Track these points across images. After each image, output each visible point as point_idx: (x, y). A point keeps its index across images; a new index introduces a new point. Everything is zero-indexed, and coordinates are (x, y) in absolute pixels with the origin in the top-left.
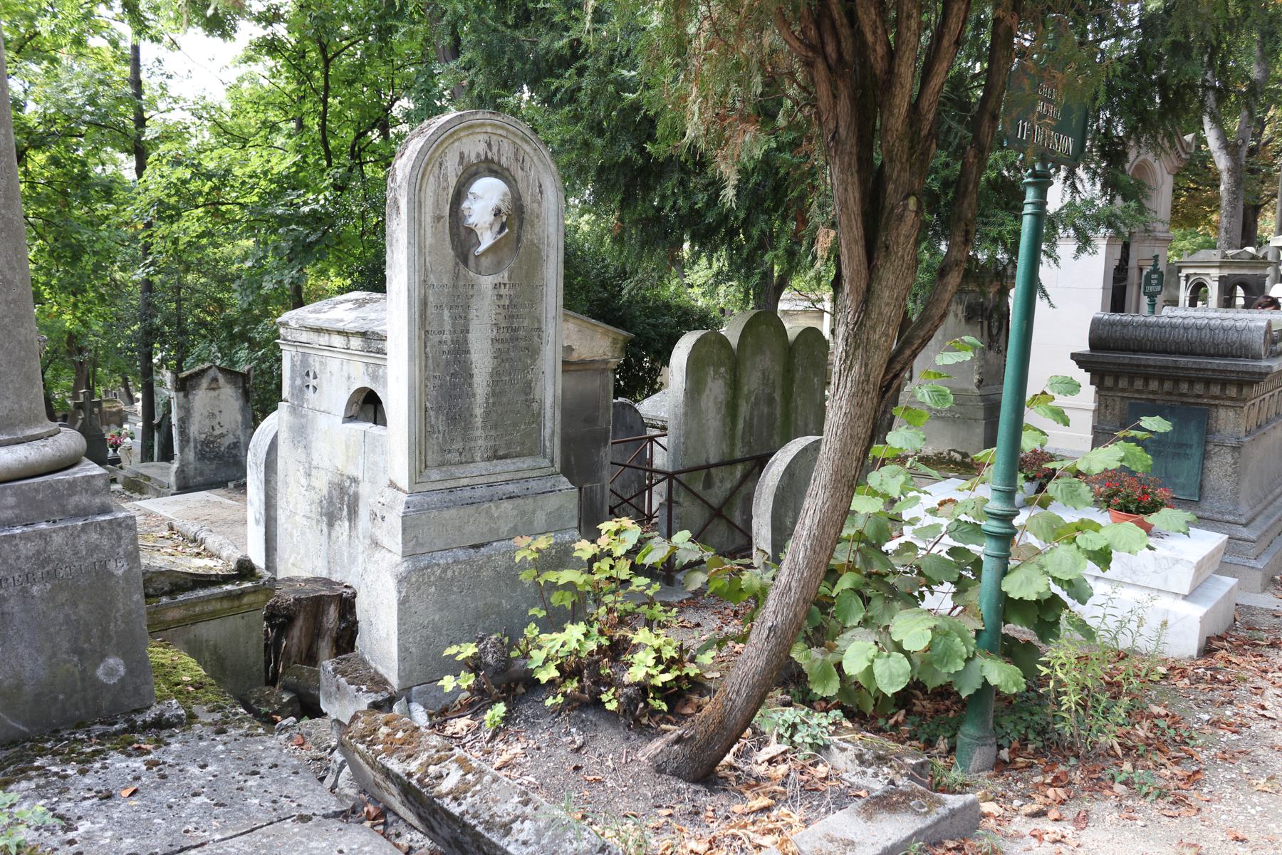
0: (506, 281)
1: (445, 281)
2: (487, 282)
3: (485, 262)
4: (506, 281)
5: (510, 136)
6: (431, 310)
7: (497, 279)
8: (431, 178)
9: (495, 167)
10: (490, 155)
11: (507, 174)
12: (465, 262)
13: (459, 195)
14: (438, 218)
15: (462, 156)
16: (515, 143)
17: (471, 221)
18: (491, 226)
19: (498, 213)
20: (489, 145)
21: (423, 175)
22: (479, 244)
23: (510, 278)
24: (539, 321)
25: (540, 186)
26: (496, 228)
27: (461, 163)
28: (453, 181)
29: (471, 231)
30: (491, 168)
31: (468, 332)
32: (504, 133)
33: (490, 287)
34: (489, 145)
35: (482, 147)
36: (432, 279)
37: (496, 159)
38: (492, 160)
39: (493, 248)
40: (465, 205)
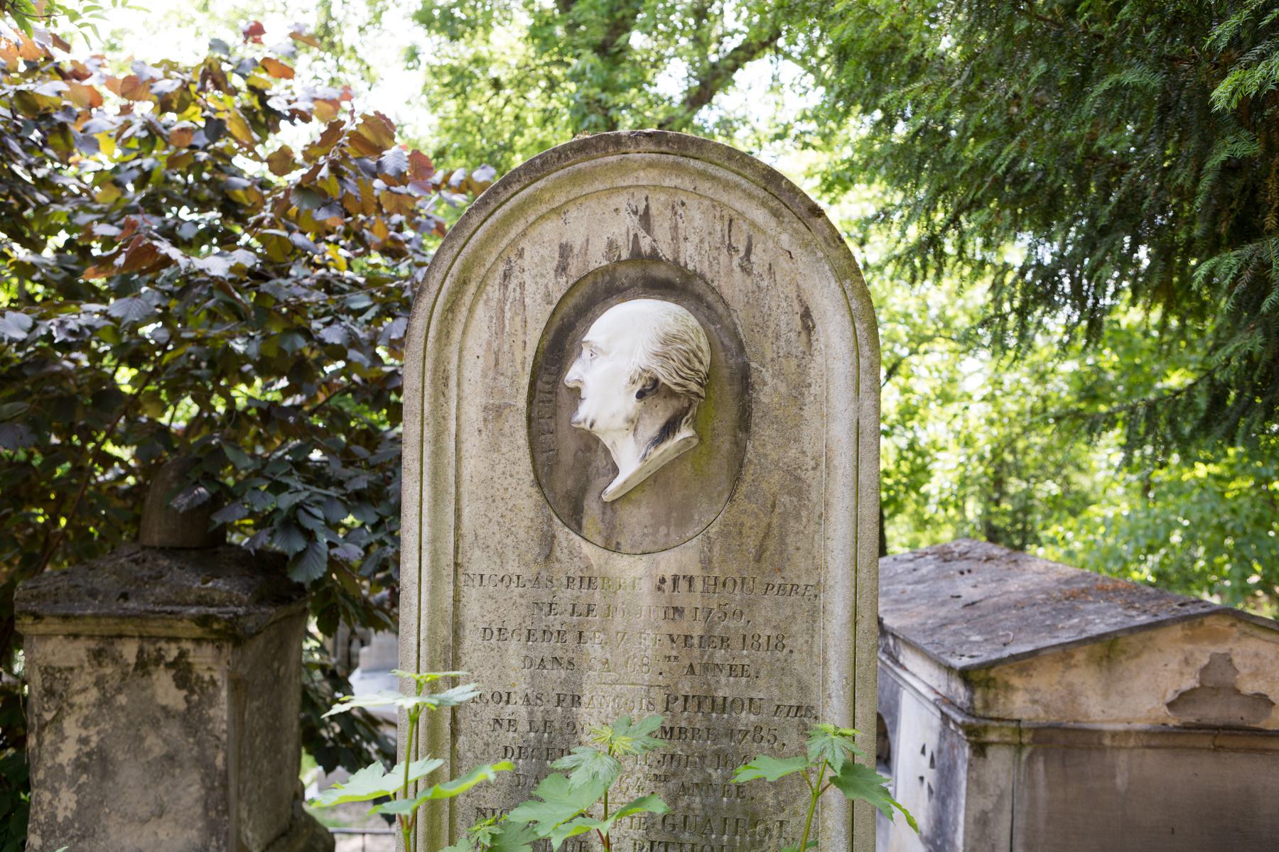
0: (695, 570)
1: (513, 567)
2: (634, 574)
3: (636, 518)
4: (695, 570)
5: (705, 187)
6: (471, 640)
7: (669, 563)
8: (480, 311)
9: (660, 272)
11: (699, 286)
12: (575, 519)
13: (559, 345)
14: (495, 412)
15: (565, 250)
16: (715, 204)
17: (585, 412)
18: (633, 423)
19: (650, 390)
20: (645, 219)
21: (451, 308)
22: (615, 471)
23: (706, 563)
24: (803, 688)
25: (806, 315)
26: (651, 427)
27: (562, 269)
28: (538, 316)
29: (590, 442)
31: (576, 700)
32: (686, 183)
33: (646, 587)
34: (645, 219)
35: (621, 227)
36: (477, 561)
37: (665, 251)
38: (654, 257)
39: (655, 481)
40: (573, 374)
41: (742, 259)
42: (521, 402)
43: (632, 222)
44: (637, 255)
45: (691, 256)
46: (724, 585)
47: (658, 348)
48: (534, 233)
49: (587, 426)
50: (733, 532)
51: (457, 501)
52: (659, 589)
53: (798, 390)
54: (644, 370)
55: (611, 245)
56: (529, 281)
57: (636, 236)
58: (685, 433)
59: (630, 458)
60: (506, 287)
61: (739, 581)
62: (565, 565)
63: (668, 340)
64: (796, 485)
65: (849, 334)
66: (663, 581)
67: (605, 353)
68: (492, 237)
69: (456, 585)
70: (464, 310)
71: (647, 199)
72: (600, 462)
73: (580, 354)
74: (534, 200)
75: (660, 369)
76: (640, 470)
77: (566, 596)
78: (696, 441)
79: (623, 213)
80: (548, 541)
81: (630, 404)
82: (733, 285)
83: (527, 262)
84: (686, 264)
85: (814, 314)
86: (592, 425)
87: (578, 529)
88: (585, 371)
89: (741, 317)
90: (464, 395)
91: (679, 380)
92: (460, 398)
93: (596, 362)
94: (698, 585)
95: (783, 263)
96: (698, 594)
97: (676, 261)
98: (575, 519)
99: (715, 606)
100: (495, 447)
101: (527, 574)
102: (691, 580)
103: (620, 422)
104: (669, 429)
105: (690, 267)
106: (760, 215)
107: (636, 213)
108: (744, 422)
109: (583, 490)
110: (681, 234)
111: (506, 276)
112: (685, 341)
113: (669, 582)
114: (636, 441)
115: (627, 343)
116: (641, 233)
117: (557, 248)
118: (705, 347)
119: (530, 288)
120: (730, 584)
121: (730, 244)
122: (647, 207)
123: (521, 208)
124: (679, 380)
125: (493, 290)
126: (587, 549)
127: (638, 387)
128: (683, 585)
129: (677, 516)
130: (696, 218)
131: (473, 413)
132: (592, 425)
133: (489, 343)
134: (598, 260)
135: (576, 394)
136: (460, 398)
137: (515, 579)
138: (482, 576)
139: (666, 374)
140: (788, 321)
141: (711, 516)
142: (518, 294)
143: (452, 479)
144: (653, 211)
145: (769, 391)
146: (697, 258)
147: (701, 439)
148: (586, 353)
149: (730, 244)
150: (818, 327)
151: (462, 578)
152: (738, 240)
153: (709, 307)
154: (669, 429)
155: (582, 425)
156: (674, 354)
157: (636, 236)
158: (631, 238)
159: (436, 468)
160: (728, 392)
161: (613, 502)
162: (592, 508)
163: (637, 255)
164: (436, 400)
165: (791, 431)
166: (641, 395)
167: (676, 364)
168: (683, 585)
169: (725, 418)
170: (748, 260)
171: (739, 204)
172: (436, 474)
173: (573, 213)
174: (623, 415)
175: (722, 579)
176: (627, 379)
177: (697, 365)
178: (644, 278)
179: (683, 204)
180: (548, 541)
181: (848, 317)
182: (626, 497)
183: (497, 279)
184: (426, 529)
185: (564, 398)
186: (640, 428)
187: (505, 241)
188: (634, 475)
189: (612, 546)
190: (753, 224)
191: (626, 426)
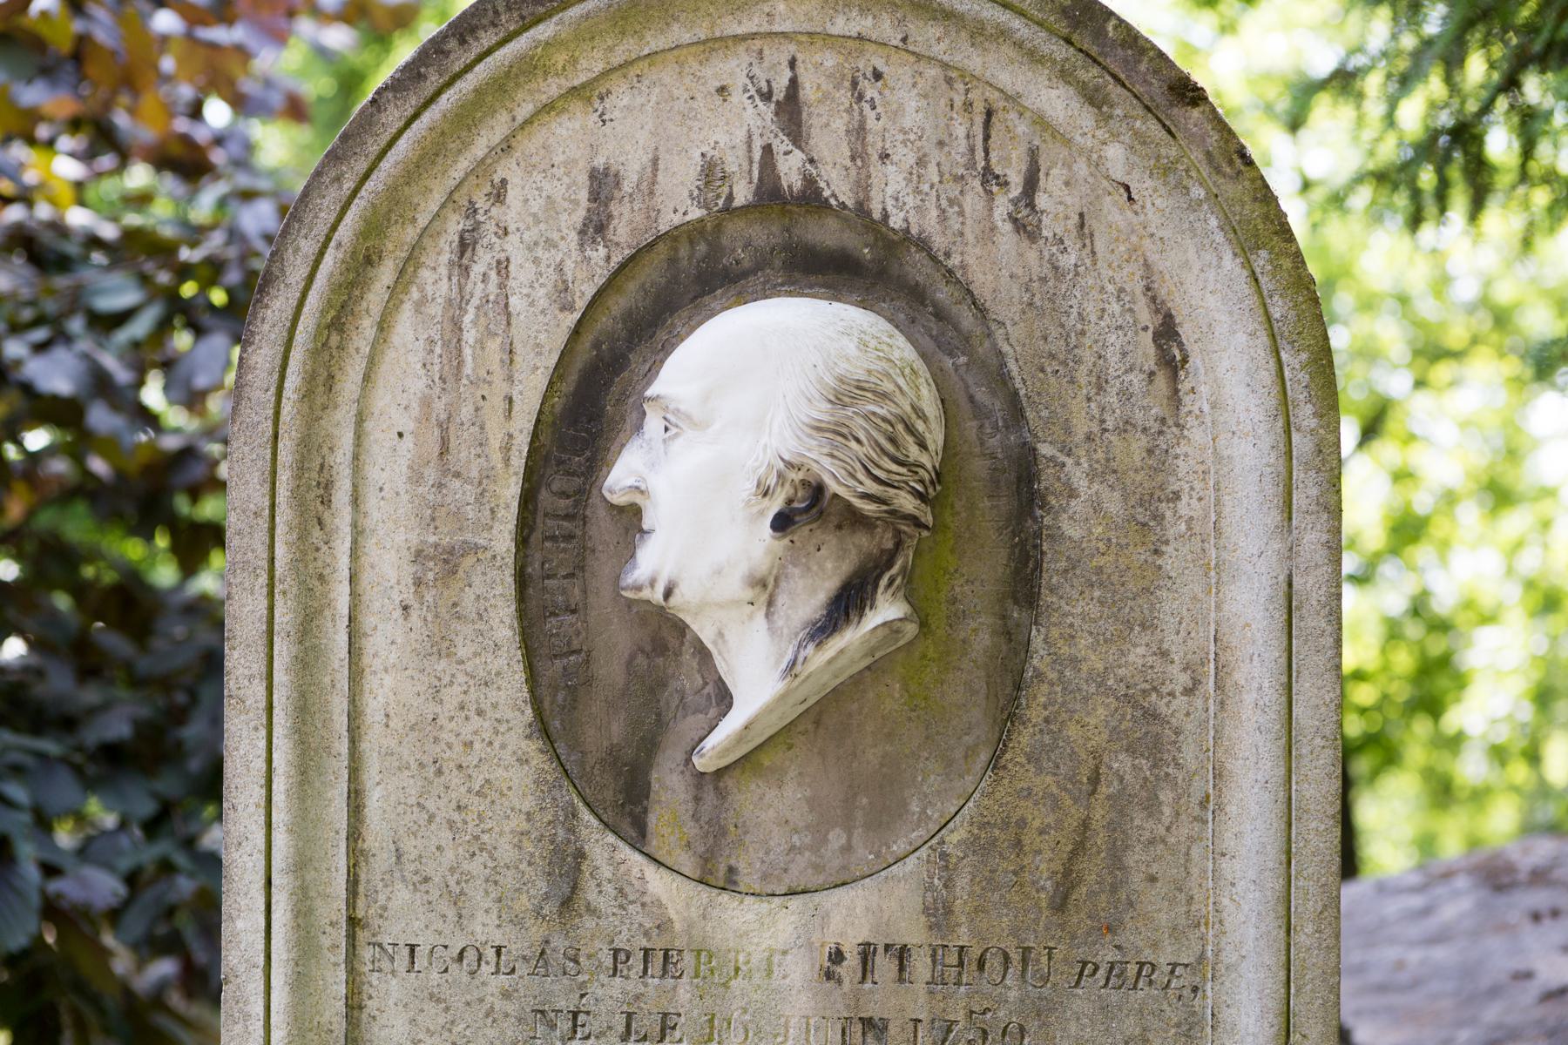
0: (913, 932)
1: (485, 928)
2: (770, 940)
4: (913, 932)
7: (852, 915)
8: (405, 326)
9: (826, 234)
10: (790, 168)
11: (916, 267)
12: (630, 814)
13: (589, 407)
14: (442, 563)
15: (602, 184)
16: (951, 75)
17: (652, 563)
18: (766, 588)
19: (804, 510)
20: (790, 111)
21: (338, 321)
22: (724, 699)
23: (939, 914)
26: (808, 598)
27: (596, 228)
30: (803, 242)
33: (798, 971)
34: (790, 111)
35: (733, 130)
36: (402, 914)
37: (837, 185)
38: (812, 199)
40: (623, 474)
41: (1015, 202)
42: (503, 540)
43: (758, 118)
44: (770, 195)
45: (896, 196)
46: (981, 965)
47: (821, 411)
48: (528, 145)
49: (657, 596)
50: (1001, 840)
51: (354, 772)
52: (829, 975)
53: (1150, 508)
54: (790, 465)
55: (711, 172)
56: (518, 256)
57: (768, 150)
58: (887, 610)
59: (757, 672)
60: (465, 271)
61: (1015, 957)
62: (607, 923)
63: (846, 393)
64: (1149, 733)
65: (1267, 376)
66: (837, 956)
67: (699, 425)
68: (431, 156)
69: (351, 970)
70: (367, 326)
71: (792, 64)
72: (688, 679)
73: (639, 427)
74: (529, 68)
75: (827, 462)
76: (782, 698)
77: (609, 994)
78: (911, 629)
79: (737, 97)
80: (567, 871)
81: (757, 543)
82: (994, 264)
83: (512, 212)
84: (886, 216)
85: (1186, 331)
86: (668, 594)
87: (638, 835)
88: (653, 465)
89: (1015, 340)
90: (368, 523)
91: (871, 487)
92: (358, 532)
93: (677, 445)
94: (921, 966)
95: (1113, 212)
96: (920, 988)
97: (862, 209)
98: (630, 814)
99: (960, 1016)
100: (440, 646)
101: (519, 944)
102: (902, 955)
103: (733, 586)
104: (849, 601)
105: (896, 222)
106: (1057, 102)
107: (767, 96)
108: (1024, 584)
109: (649, 745)
110: (874, 146)
111: (465, 245)
112: (884, 396)
113: (852, 960)
114: (772, 630)
115: (751, 395)
116: (781, 144)
117: (583, 179)
118: (931, 407)
119: (521, 273)
120: (994, 962)
121: (987, 168)
122: (794, 82)
123: (501, 88)
124: (871, 487)
125: (435, 280)
126: (658, 883)
127: (776, 505)
128: (885, 966)
129: (869, 806)
130: (907, 107)
131: (389, 565)
132: (668, 594)
133: (426, 403)
134: (679, 206)
135: (630, 520)
136: (358, 532)
137: (490, 954)
138: (413, 948)
139: (841, 474)
140: (1123, 347)
141: (948, 804)
142: (492, 288)
143: (341, 722)
144: (808, 92)
145: (1083, 512)
146: (911, 201)
147: (923, 625)
148: (653, 424)
149: (987, 168)
150: (1195, 361)
151: (366, 953)
152: (1006, 160)
153: (940, 315)
154: (849, 601)
155: (646, 594)
156: (859, 426)
157: (768, 150)
158: (757, 155)
159: (303, 695)
160: (986, 514)
161: (720, 773)
162: (669, 788)
163: (770, 195)
164: (303, 535)
165: (1133, 602)
166: (782, 523)
167: (867, 450)
168: (885, 966)
169: (979, 575)
170: (1031, 205)
171: (1008, 74)
172: (304, 709)
173: (621, 97)
174: (742, 569)
175: (975, 952)
176: (750, 486)
177: (914, 452)
178: (787, 247)
179: (878, 76)
180: (567, 871)
181: (1263, 339)
182: (749, 761)
183: (443, 252)
184: (280, 839)
185: (602, 529)
186: (782, 599)
187: (464, 164)
188: (768, 710)
189: (716, 876)
190: (1041, 122)
191: (749, 594)
